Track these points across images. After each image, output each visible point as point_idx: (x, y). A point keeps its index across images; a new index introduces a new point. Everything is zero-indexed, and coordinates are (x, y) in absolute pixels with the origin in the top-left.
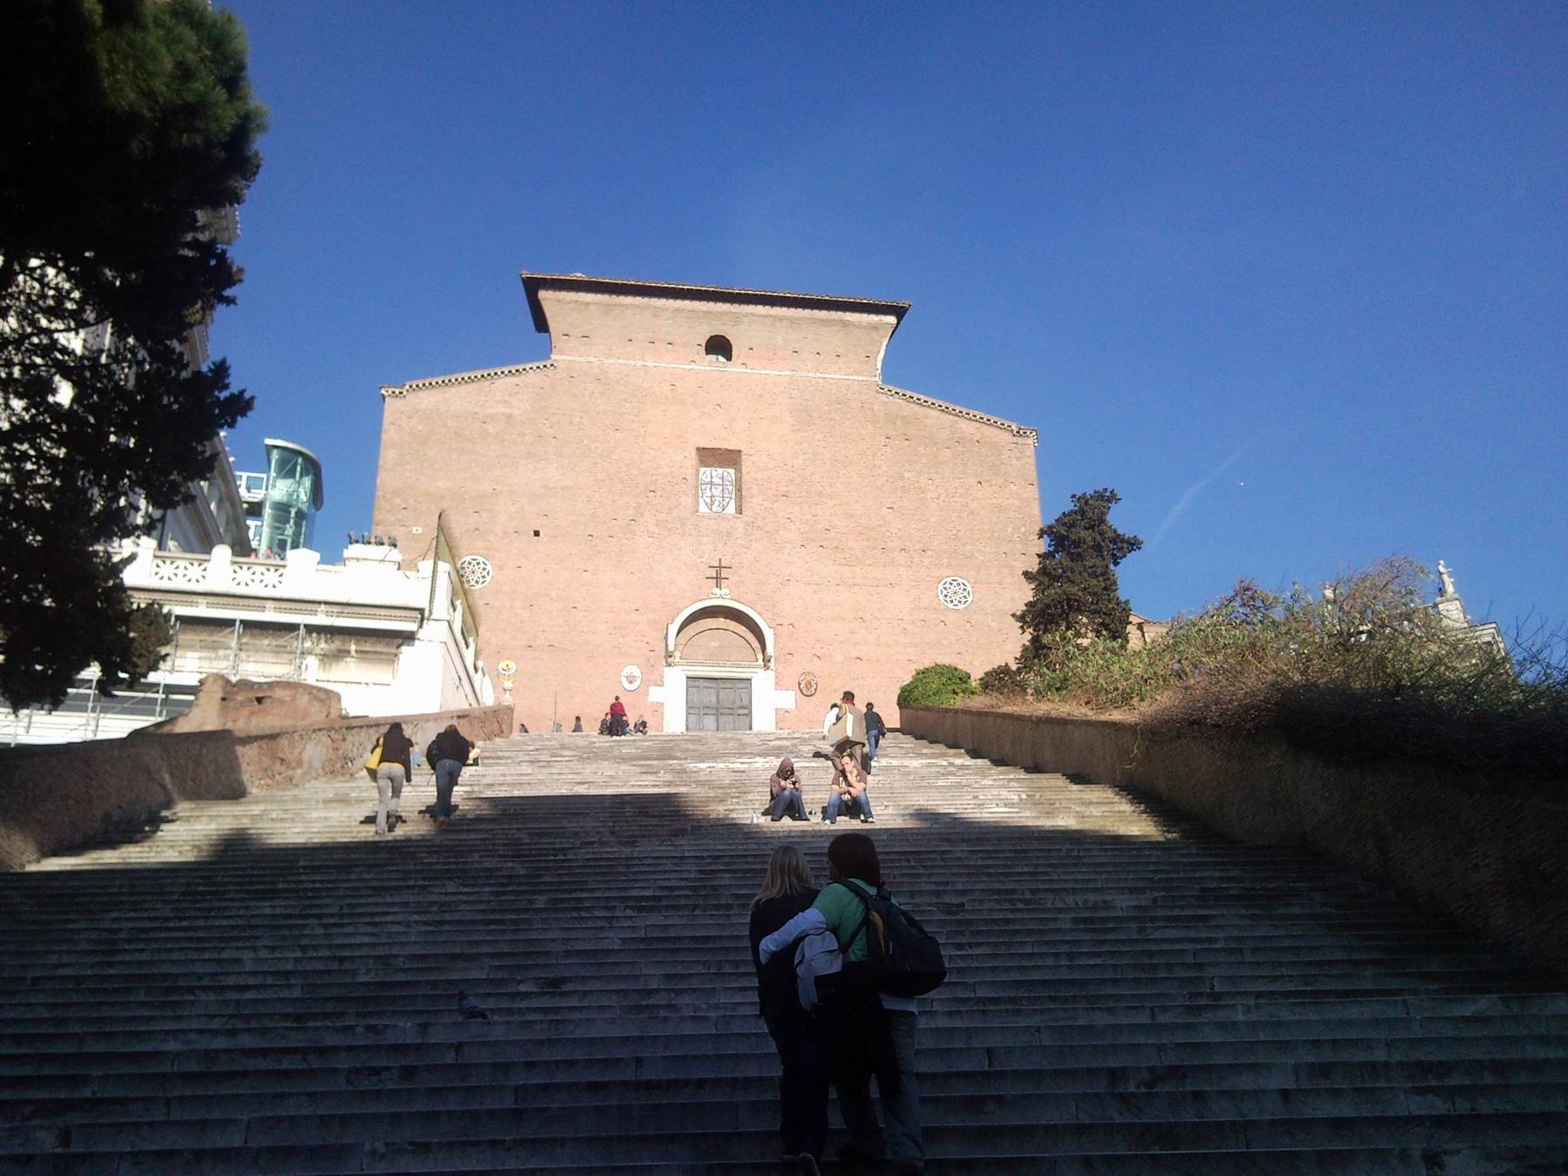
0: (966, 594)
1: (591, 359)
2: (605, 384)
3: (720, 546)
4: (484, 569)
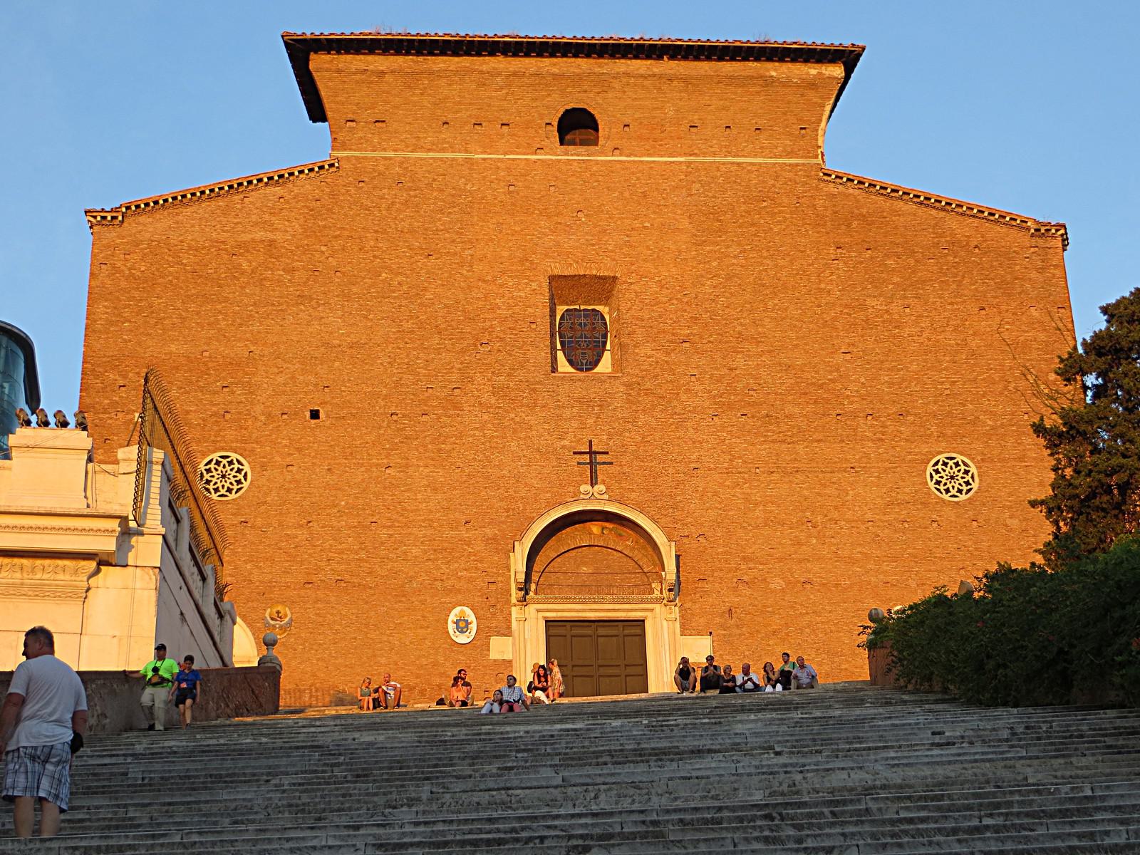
0: (968, 478)
1: (391, 154)
2: (410, 189)
3: (590, 421)
4: (239, 471)
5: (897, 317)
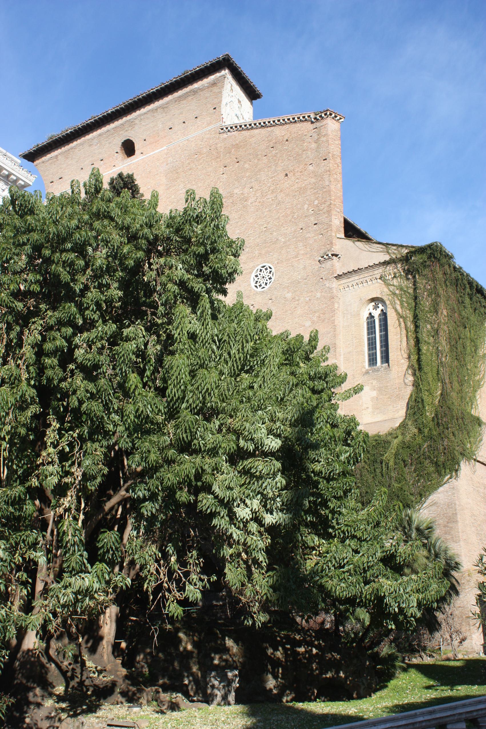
5: (246, 195)
